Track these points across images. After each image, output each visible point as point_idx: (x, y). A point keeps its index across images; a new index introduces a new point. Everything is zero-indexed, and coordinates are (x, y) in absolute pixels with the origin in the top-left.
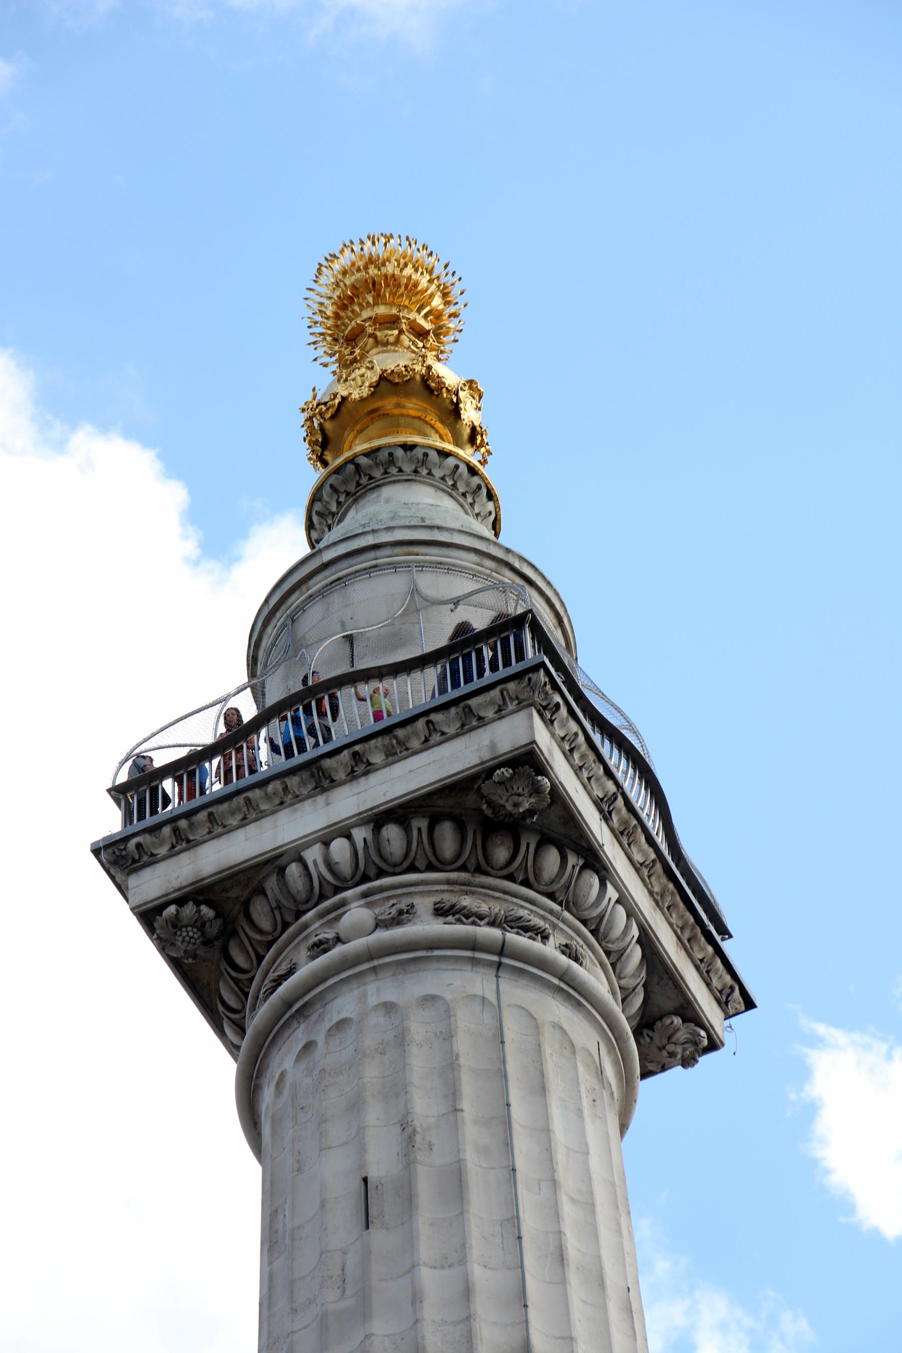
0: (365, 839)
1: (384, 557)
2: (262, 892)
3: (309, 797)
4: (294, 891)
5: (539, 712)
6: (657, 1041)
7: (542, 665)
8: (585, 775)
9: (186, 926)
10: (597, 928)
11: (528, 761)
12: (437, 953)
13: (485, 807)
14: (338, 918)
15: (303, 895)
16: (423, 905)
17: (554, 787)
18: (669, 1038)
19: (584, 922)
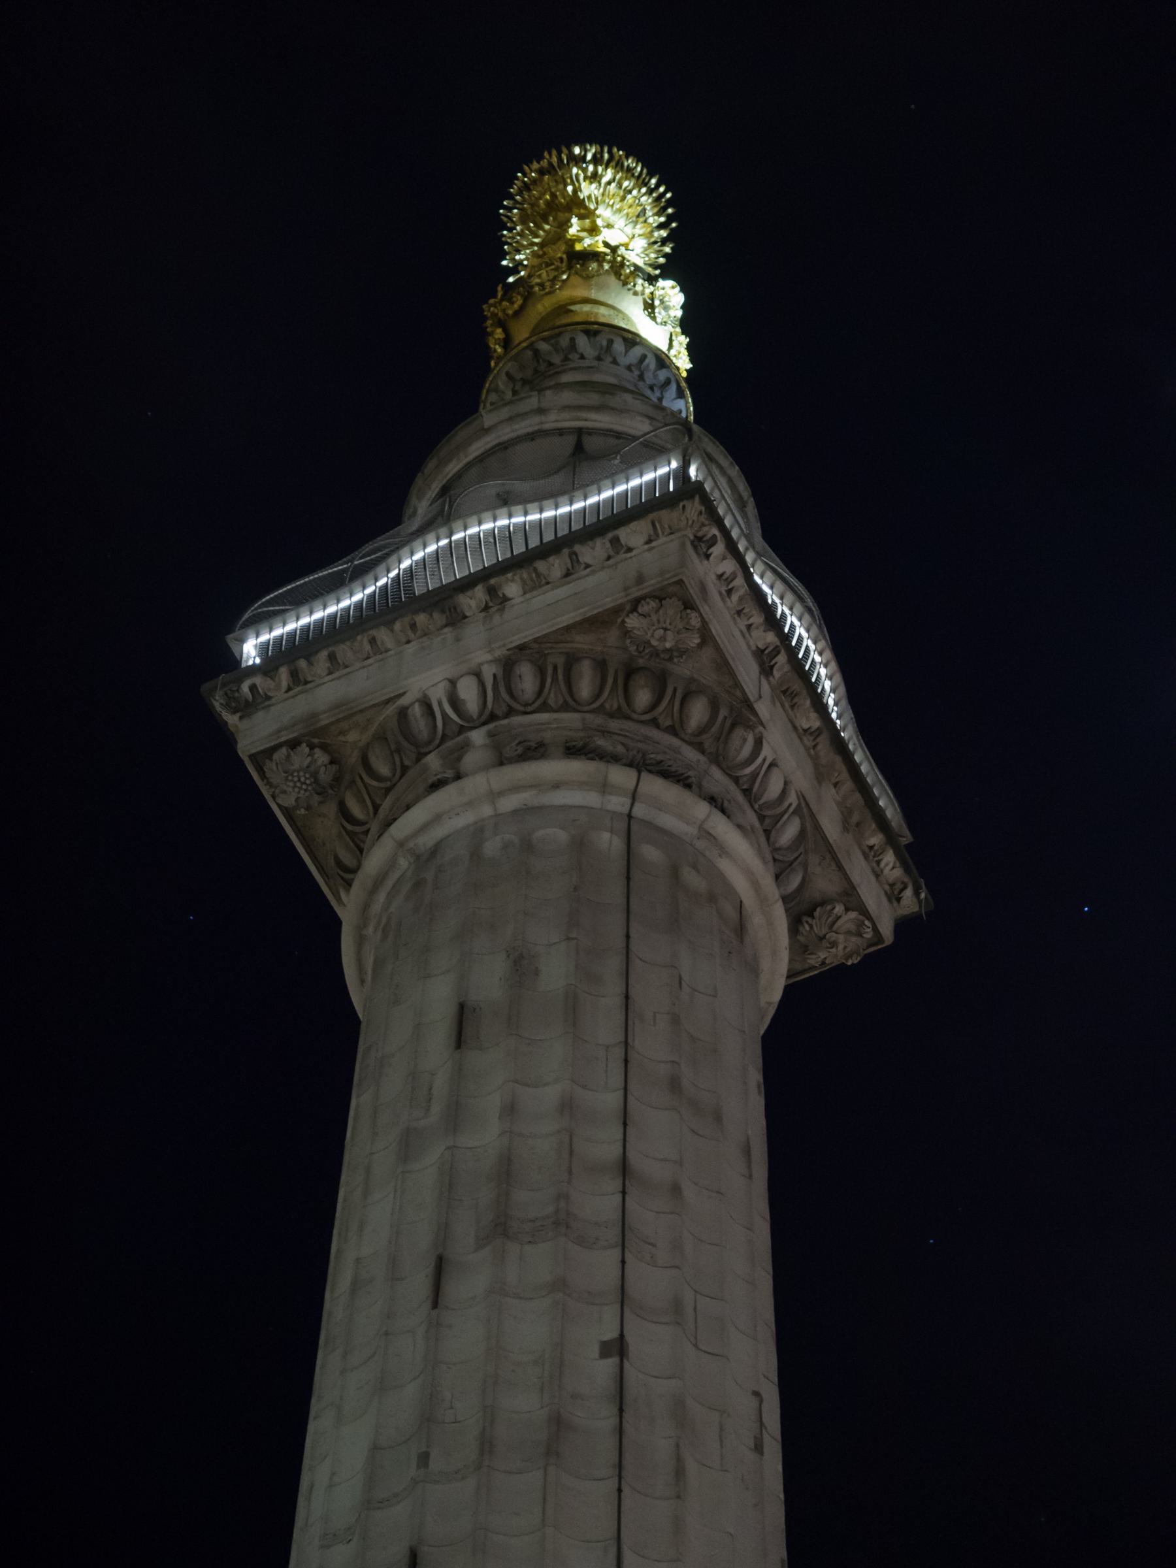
0: (495, 676)
5: (692, 542)
19: (736, 780)
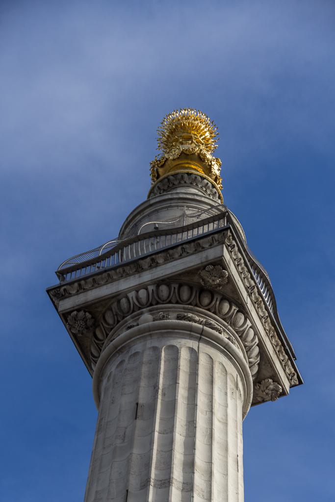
0: (153, 290)
1: (174, 203)
2: (110, 309)
3: (133, 274)
4: (122, 308)
5: (226, 246)
6: (262, 388)
7: (230, 228)
8: (243, 276)
9: (80, 320)
10: (242, 335)
11: (220, 263)
12: (176, 331)
13: (201, 280)
14: (138, 319)
15: (126, 310)
17: (229, 275)
18: (267, 387)
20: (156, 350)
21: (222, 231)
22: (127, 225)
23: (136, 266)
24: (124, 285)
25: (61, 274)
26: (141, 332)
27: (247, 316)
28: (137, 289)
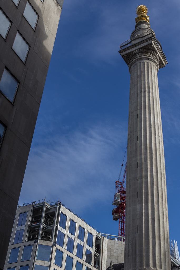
2: (131, 54)
3: (135, 47)
10: (156, 57)
11: (151, 44)
16: (143, 55)
20: (140, 63)
21: (151, 37)
22: (132, 34)
23: (135, 45)
24: (133, 49)
25: (121, 47)
26: (137, 59)
27: (157, 53)
28: (136, 50)
